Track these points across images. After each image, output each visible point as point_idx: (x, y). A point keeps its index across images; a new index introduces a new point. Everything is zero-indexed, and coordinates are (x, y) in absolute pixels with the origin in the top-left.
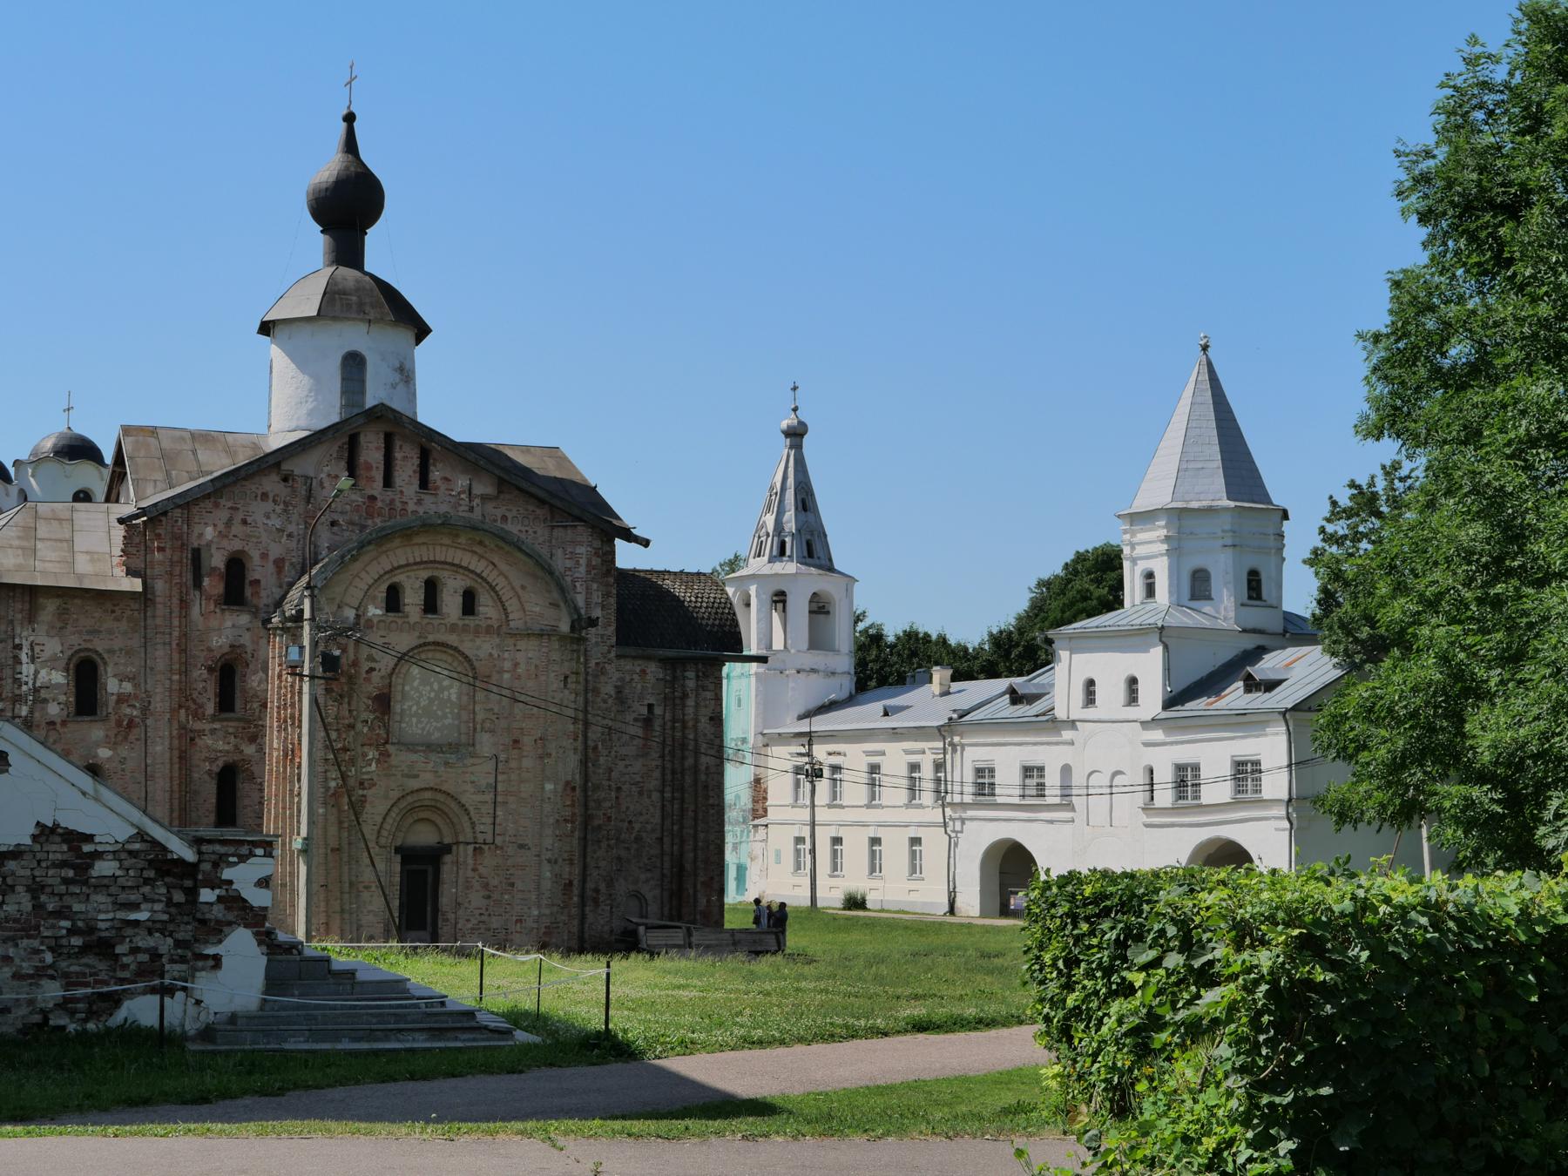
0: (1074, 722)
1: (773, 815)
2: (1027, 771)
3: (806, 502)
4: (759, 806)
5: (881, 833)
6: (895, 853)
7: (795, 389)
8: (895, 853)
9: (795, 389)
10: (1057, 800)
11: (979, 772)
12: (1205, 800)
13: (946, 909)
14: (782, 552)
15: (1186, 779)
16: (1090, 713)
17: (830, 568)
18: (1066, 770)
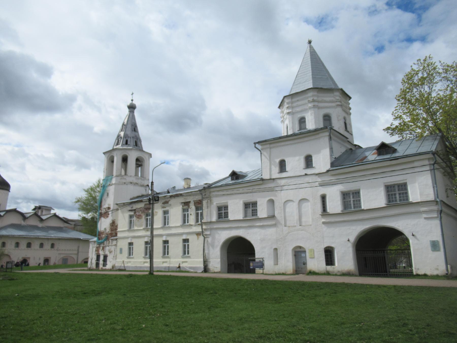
0: (274, 179)
1: (119, 235)
2: (246, 205)
3: (135, 129)
4: (114, 232)
5: (168, 239)
6: (176, 247)
7: (132, 94)
8: (176, 247)
9: (132, 94)
10: (265, 216)
11: (219, 208)
12: (364, 206)
13: (203, 270)
14: (127, 143)
15: (351, 200)
16: (284, 175)
17: (142, 150)
18: (271, 202)
